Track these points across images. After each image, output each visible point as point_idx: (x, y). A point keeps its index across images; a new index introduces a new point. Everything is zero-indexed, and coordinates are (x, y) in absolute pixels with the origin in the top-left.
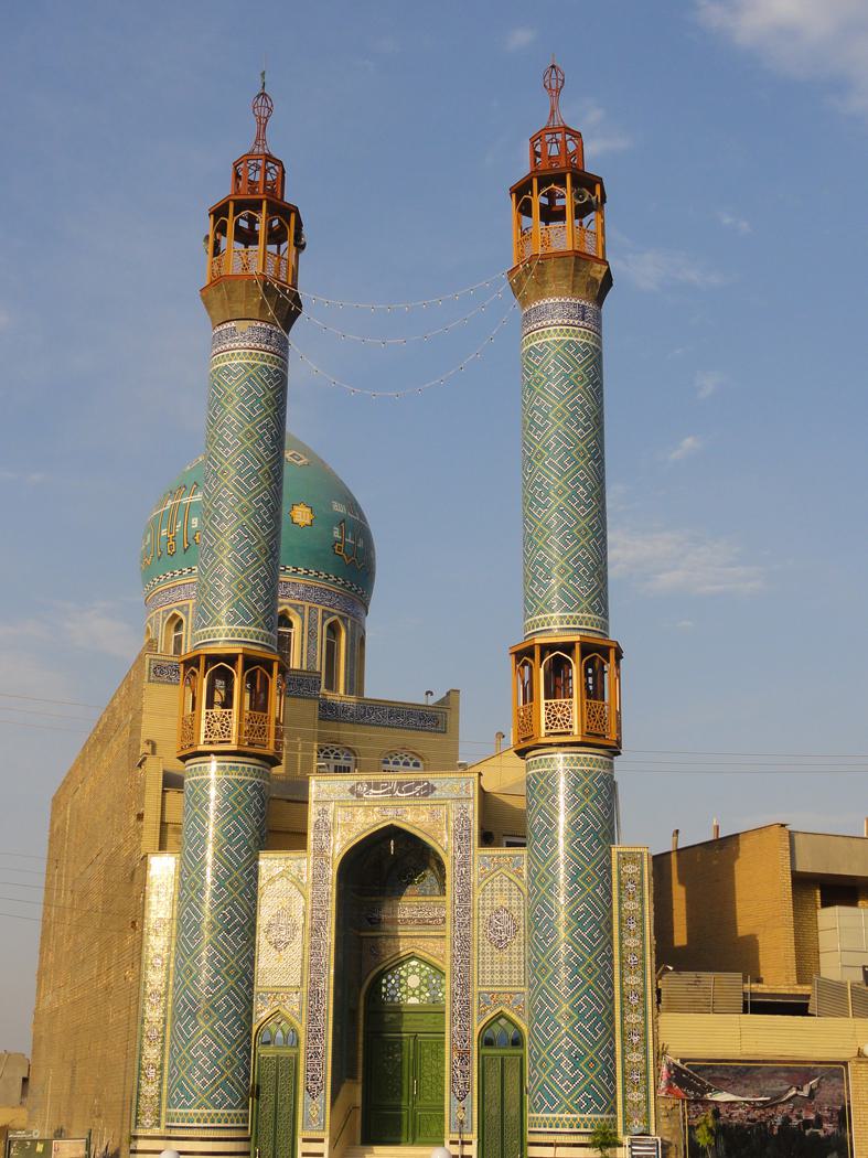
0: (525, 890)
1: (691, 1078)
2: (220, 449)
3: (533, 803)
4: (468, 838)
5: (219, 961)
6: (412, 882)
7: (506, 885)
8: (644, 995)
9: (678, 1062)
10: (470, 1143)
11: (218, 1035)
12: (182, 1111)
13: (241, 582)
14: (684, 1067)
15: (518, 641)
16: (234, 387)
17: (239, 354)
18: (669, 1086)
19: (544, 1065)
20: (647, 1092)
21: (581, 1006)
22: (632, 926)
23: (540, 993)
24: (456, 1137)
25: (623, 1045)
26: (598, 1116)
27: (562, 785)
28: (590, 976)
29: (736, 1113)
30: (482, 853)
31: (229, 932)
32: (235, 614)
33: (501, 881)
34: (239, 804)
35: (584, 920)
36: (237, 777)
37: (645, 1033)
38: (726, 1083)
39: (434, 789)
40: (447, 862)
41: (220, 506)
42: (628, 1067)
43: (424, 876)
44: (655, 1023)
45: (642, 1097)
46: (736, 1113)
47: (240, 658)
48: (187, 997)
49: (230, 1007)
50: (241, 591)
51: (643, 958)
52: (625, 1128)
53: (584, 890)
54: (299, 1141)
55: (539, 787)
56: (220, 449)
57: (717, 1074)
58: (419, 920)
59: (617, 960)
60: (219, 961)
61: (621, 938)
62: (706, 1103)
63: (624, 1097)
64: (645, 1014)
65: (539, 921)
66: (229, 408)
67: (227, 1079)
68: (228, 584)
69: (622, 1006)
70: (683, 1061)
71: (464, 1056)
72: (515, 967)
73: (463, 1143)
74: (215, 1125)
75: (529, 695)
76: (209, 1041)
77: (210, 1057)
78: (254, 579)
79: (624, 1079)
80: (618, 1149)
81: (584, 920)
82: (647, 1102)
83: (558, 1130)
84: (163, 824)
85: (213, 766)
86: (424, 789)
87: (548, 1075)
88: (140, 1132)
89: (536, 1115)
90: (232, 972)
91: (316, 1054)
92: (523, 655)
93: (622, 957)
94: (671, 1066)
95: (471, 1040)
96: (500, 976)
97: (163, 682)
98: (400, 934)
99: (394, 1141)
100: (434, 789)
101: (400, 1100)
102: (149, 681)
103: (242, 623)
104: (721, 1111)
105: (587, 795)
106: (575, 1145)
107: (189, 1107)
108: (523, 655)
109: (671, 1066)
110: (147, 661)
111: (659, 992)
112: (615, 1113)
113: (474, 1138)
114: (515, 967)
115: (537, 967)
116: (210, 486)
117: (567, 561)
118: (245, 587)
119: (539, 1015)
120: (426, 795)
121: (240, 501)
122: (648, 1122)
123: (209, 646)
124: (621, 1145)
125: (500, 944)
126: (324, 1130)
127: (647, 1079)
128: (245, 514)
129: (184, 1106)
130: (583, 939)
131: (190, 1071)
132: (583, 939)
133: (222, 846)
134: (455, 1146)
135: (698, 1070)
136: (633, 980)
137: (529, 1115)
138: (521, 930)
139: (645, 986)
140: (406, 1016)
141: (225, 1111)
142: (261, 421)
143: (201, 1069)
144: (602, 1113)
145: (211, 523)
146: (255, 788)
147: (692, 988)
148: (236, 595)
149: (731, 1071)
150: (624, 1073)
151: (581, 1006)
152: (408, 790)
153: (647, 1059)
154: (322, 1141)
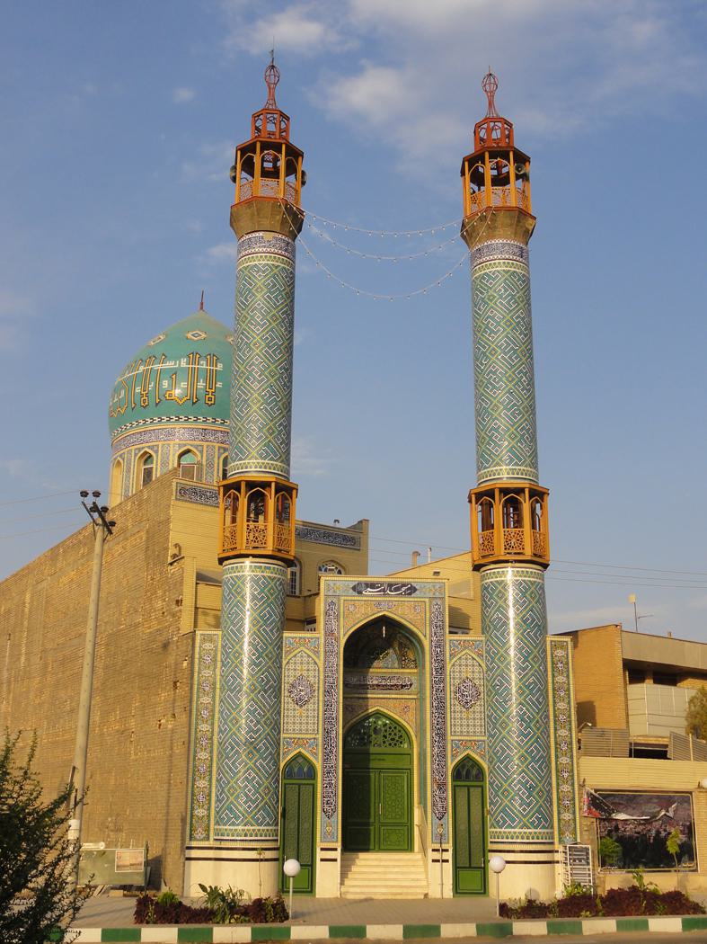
0: (483, 665)
1: (603, 803)
2: (252, 327)
3: (492, 603)
4: (443, 628)
5: (259, 714)
6: (377, 658)
7: (470, 662)
8: (571, 743)
9: (593, 792)
10: (447, 850)
11: (259, 770)
12: (231, 827)
13: (270, 428)
14: (596, 795)
15: (473, 485)
16: (260, 280)
17: (266, 256)
18: (589, 808)
19: (506, 793)
20: (574, 813)
21: (532, 751)
22: (562, 694)
23: (502, 741)
24: (437, 846)
25: (557, 779)
26: (546, 831)
27: (511, 595)
28: (538, 729)
29: (628, 828)
30: (452, 638)
31: (266, 692)
32: (267, 452)
33: (466, 659)
34: (272, 595)
35: (534, 688)
36: (269, 575)
37: (572, 771)
38: (622, 807)
39: (415, 590)
40: (426, 643)
41: (254, 369)
42: (561, 794)
43: (387, 654)
44: (578, 763)
45: (571, 816)
46: (628, 828)
47: (273, 485)
48: (234, 740)
49: (267, 749)
50: (271, 435)
51: (570, 716)
52: (560, 839)
53: (533, 667)
54: (318, 850)
55: (490, 596)
56: (252, 327)
57: (617, 800)
58: (383, 686)
59: (552, 718)
60: (259, 714)
61: (554, 702)
62: (610, 820)
63: (559, 817)
64: (572, 757)
65: (496, 687)
66: (259, 296)
67: (266, 803)
68: (260, 430)
69: (556, 751)
70: (596, 791)
71: (441, 786)
72: (478, 723)
73: (443, 850)
74: (263, 838)
75: (487, 525)
76: (253, 774)
77: (253, 786)
78: (279, 426)
79: (559, 804)
80: (556, 854)
81: (534, 688)
82: (575, 820)
83: (499, 840)
84: (196, 608)
85: (247, 568)
86: (408, 589)
87: (510, 801)
88: (194, 844)
89: (498, 830)
90: (268, 722)
91: (330, 784)
92: (483, 498)
93: (555, 716)
94: (590, 795)
95: (446, 773)
96: (466, 729)
97: (186, 501)
98: (369, 696)
99: (367, 850)
100: (415, 590)
101: (369, 818)
102: (176, 499)
103: (272, 459)
104: (620, 827)
105: (533, 599)
106: (522, 852)
107: (238, 825)
108: (483, 498)
109: (590, 795)
110: (174, 484)
111: (579, 741)
112: (552, 827)
113: (450, 846)
114: (478, 723)
115: (494, 722)
116: (244, 354)
117: (516, 430)
118: (274, 432)
119: (498, 757)
120: (410, 594)
121: (269, 367)
122: (575, 834)
123: (246, 474)
124: (557, 852)
125: (467, 705)
126: (337, 841)
127: (574, 804)
128: (273, 377)
129: (233, 824)
130: (533, 703)
131: (237, 797)
132: (533, 703)
133: (261, 626)
134: (436, 853)
135: (605, 797)
136: (563, 732)
137: (490, 830)
138: (482, 695)
139: (571, 737)
140: (372, 757)
141: (265, 828)
142: (282, 309)
143: (247, 795)
144: (547, 828)
145: (246, 382)
146: (281, 584)
147: (599, 739)
148: (267, 437)
149: (625, 798)
150: (559, 799)
151: (532, 751)
152: (396, 590)
153: (573, 789)
154: (335, 849)
